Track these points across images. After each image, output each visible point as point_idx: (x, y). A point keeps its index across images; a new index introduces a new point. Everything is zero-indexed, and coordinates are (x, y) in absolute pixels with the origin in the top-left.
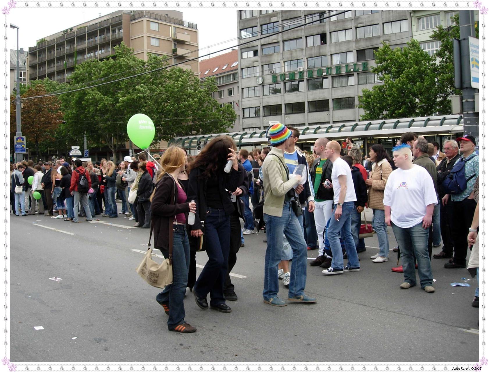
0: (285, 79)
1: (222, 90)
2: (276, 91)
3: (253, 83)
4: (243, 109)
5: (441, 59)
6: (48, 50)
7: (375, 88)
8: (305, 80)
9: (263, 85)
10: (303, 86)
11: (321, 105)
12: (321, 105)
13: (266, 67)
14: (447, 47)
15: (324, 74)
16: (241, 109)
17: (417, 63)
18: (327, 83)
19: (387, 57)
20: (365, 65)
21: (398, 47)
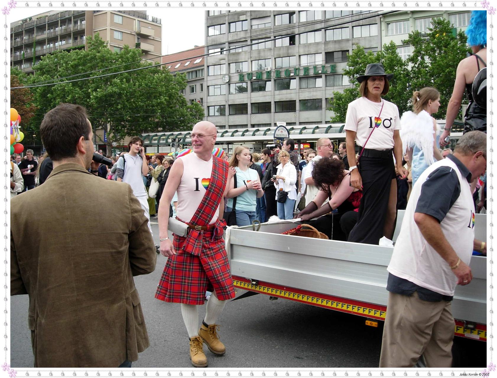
0: (252, 78)
1: (194, 84)
2: (241, 90)
3: (219, 82)
4: (208, 107)
5: (413, 65)
6: (73, 35)
7: (347, 90)
8: (272, 80)
9: (229, 83)
10: (270, 86)
11: (288, 106)
12: (288, 106)
13: (233, 66)
14: (418, 53)
15: (292, 74)
16: (205, 108)
17: (392, 68)
18: (294, 83)
19: (360, 61)
20: (334, 68)
21: (369, 51)
